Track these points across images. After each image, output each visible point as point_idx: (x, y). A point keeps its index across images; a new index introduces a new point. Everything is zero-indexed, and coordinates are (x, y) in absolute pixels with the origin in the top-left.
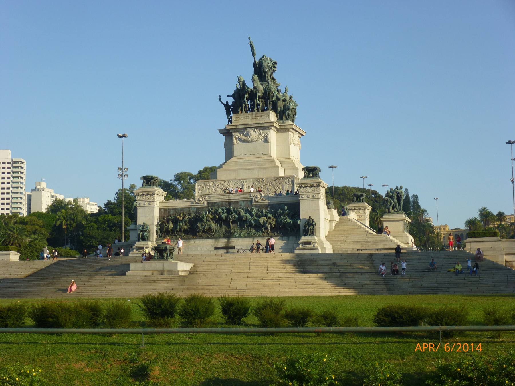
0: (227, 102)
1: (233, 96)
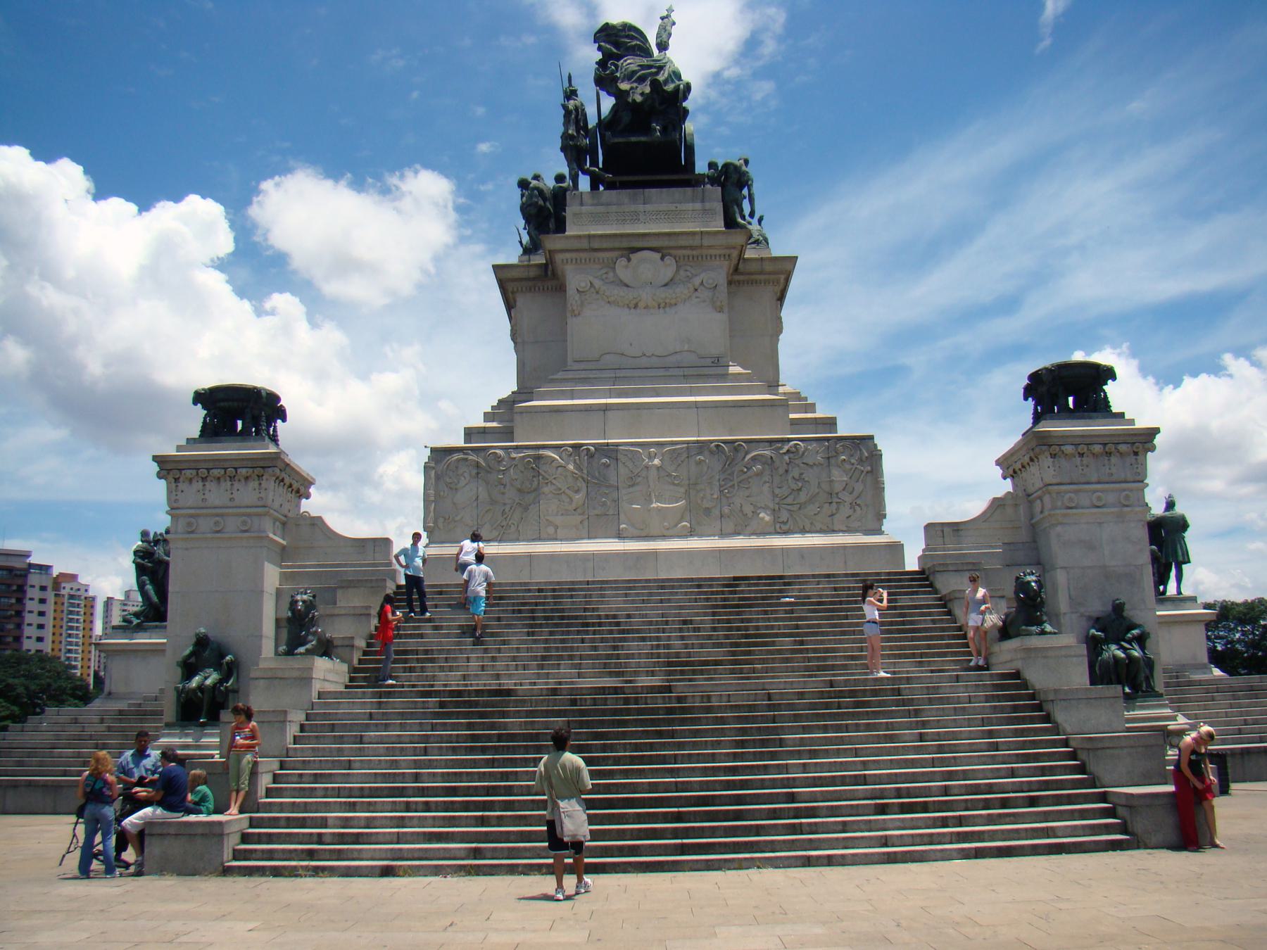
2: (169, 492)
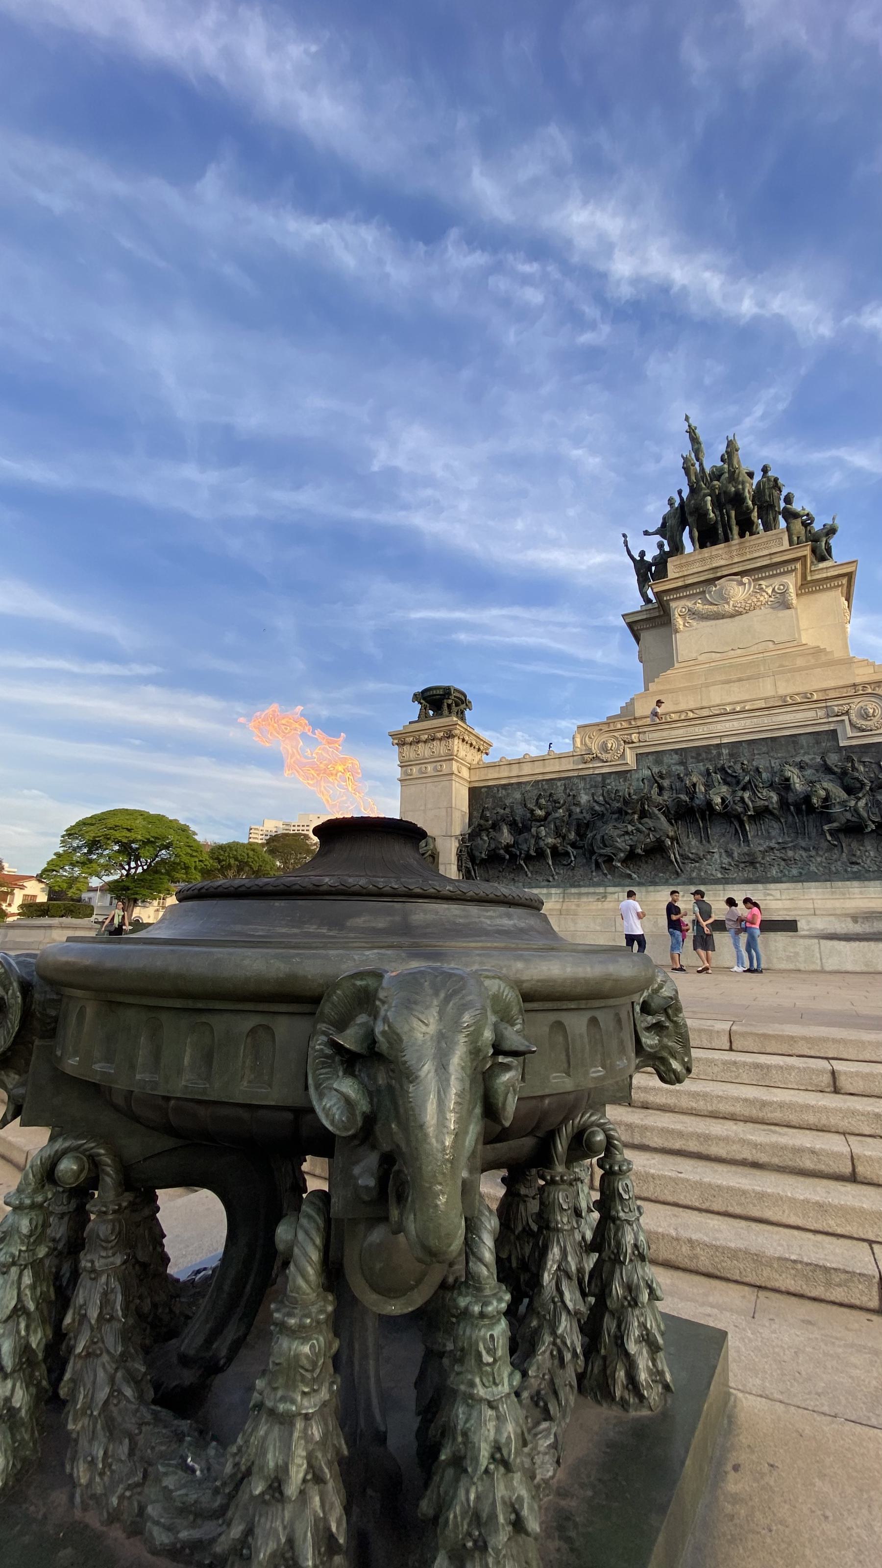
0: (642, 554)
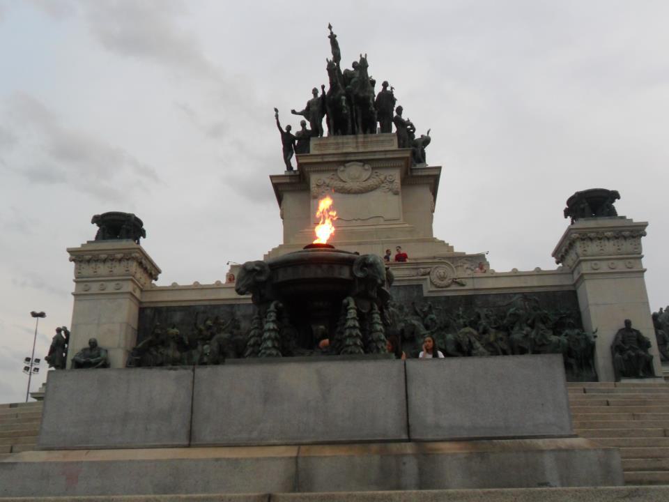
0: (289, 128)
1: (306, 113)
2: (76, 268)
